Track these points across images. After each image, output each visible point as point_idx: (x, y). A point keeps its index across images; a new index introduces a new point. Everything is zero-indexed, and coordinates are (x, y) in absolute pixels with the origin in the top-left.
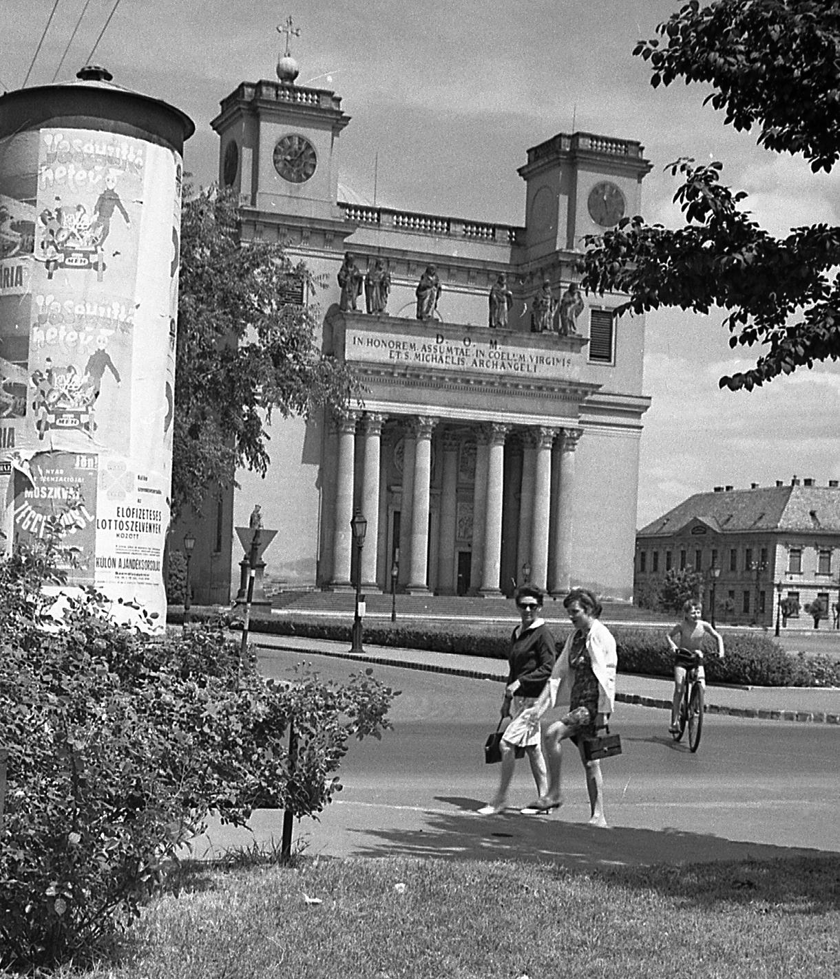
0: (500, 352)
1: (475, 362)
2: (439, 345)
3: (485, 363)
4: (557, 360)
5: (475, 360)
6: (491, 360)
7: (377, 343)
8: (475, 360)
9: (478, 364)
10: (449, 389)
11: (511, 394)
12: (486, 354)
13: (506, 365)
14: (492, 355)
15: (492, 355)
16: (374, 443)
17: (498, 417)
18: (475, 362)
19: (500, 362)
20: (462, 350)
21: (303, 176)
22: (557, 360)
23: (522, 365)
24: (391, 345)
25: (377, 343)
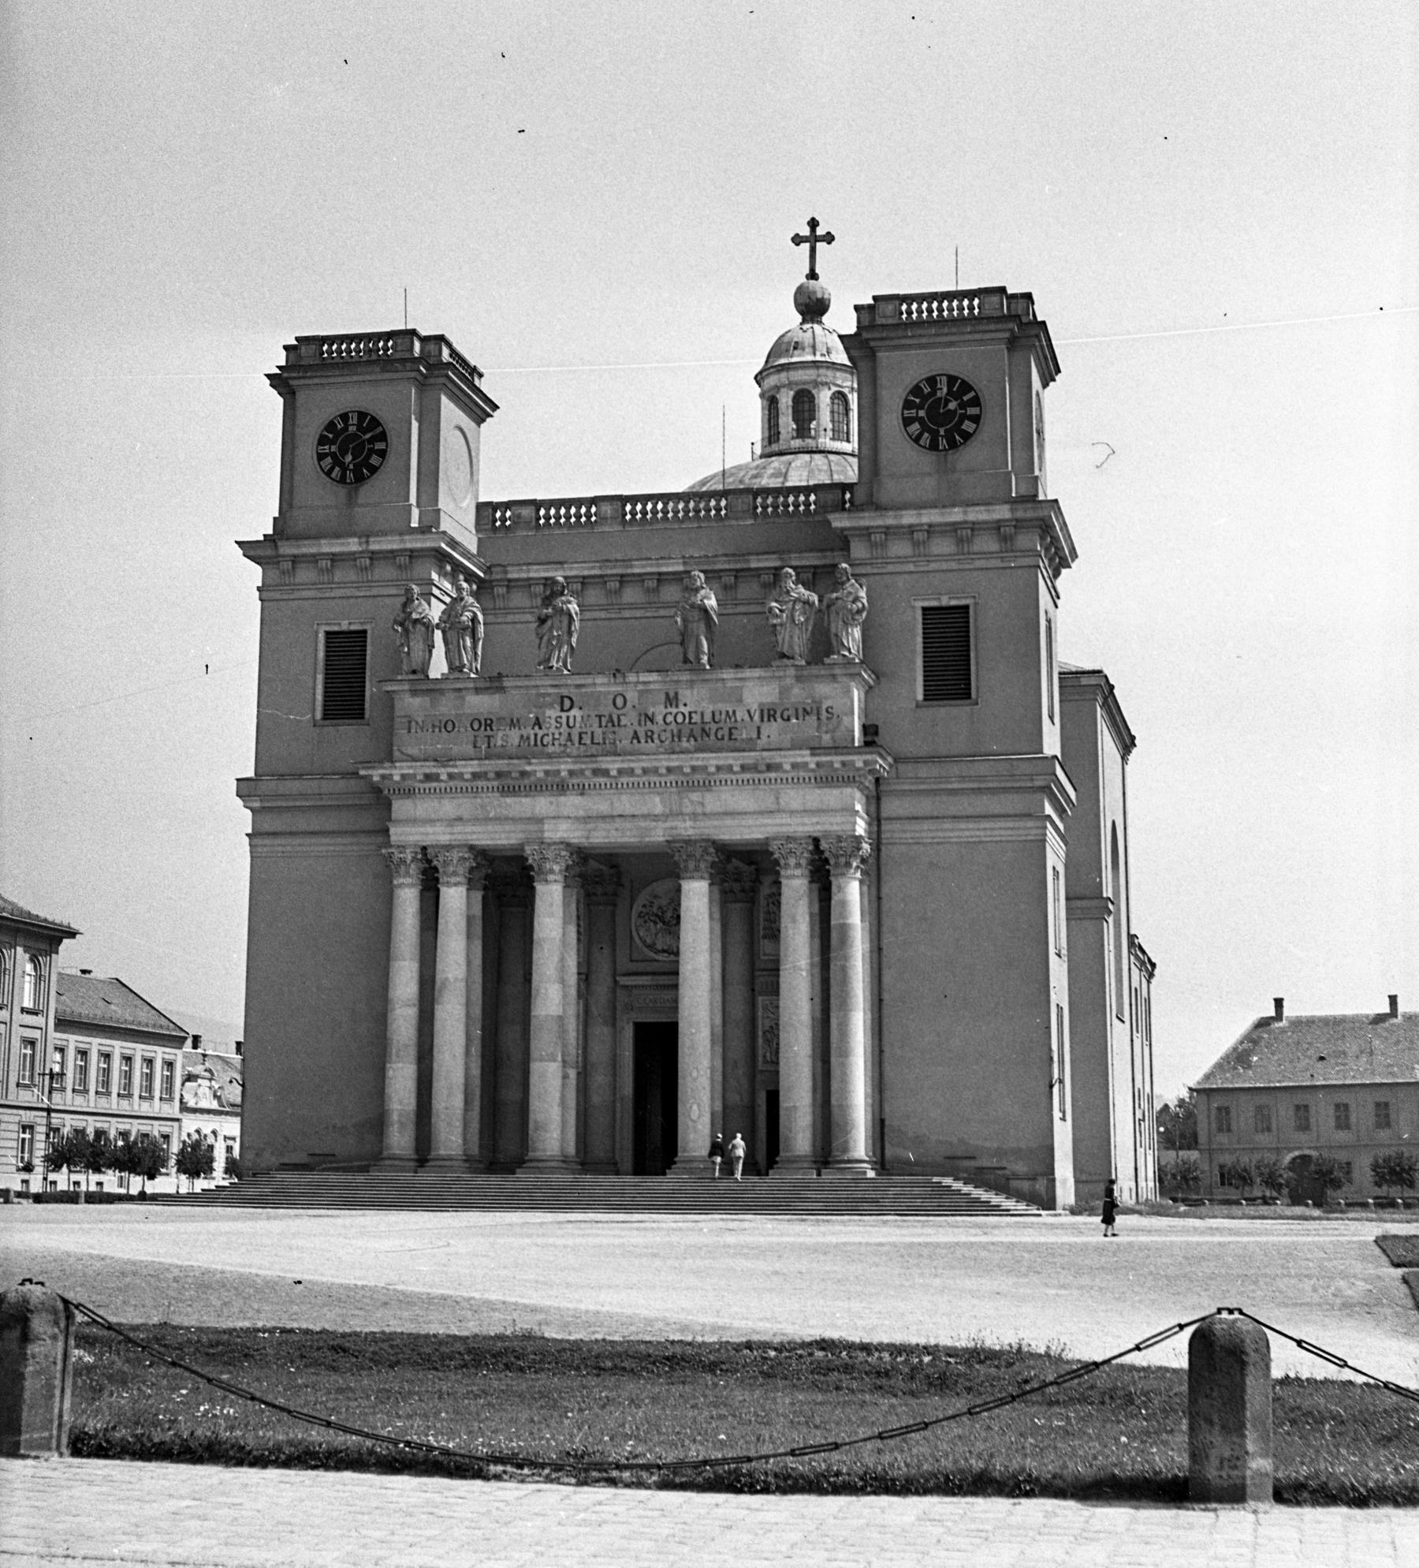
0: (685, 710)
1: (636, 736)
2: (564, 715)
3: (655, 736)
4: (805, 710)
5: (635, 732)
6: (669, 728)
7: (449, 728)
8: (635, 732)
9: (643, 741)
10: (582, 791)
11: (707, 786)
12: (659, 718)
13: (697, 732)
14: (670, 719)
15: (670, 719)
16: (455, 899)
17: (686, 829)
18: (636, 736)
19: (686, 731)
20: (611, 716)
21: (957, 439)
22: (805, 710)
23: (730, 729)
24: (476, 726)
25: (449, 728)
